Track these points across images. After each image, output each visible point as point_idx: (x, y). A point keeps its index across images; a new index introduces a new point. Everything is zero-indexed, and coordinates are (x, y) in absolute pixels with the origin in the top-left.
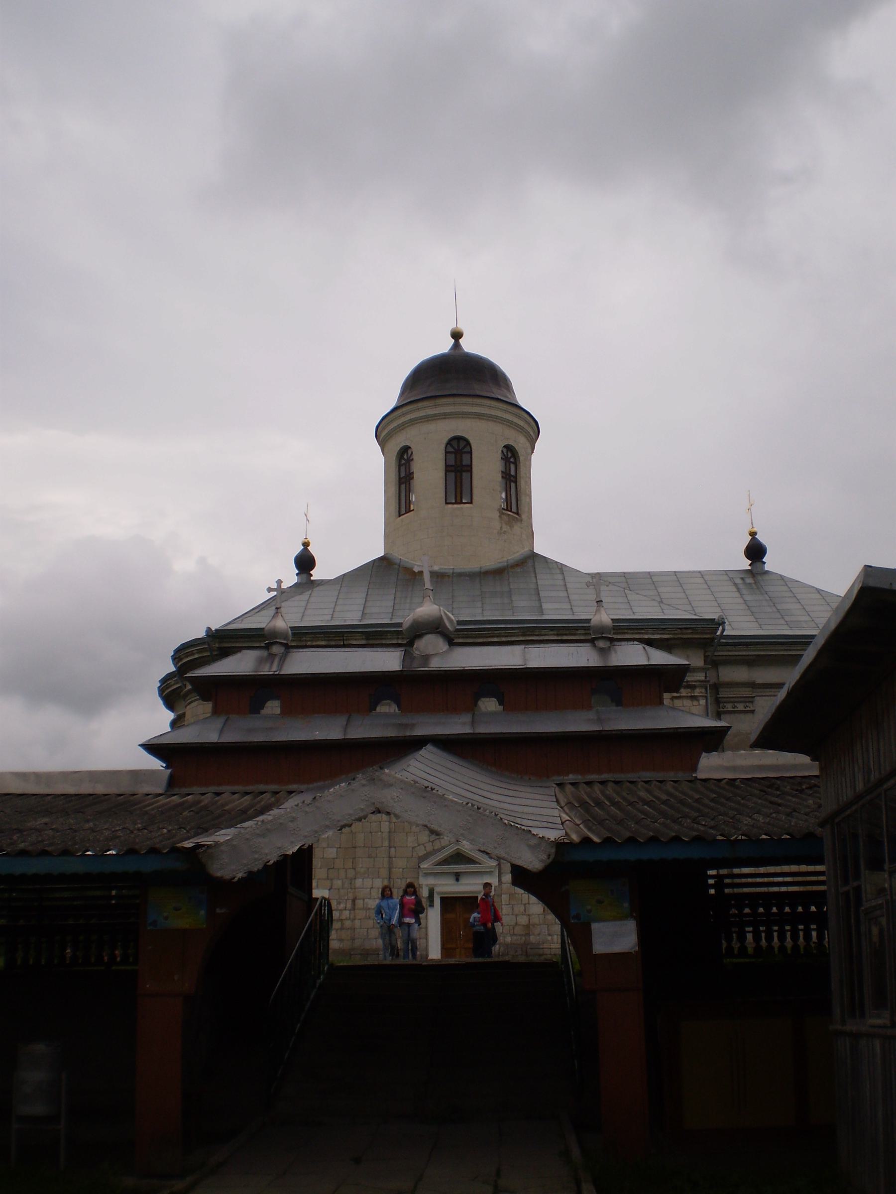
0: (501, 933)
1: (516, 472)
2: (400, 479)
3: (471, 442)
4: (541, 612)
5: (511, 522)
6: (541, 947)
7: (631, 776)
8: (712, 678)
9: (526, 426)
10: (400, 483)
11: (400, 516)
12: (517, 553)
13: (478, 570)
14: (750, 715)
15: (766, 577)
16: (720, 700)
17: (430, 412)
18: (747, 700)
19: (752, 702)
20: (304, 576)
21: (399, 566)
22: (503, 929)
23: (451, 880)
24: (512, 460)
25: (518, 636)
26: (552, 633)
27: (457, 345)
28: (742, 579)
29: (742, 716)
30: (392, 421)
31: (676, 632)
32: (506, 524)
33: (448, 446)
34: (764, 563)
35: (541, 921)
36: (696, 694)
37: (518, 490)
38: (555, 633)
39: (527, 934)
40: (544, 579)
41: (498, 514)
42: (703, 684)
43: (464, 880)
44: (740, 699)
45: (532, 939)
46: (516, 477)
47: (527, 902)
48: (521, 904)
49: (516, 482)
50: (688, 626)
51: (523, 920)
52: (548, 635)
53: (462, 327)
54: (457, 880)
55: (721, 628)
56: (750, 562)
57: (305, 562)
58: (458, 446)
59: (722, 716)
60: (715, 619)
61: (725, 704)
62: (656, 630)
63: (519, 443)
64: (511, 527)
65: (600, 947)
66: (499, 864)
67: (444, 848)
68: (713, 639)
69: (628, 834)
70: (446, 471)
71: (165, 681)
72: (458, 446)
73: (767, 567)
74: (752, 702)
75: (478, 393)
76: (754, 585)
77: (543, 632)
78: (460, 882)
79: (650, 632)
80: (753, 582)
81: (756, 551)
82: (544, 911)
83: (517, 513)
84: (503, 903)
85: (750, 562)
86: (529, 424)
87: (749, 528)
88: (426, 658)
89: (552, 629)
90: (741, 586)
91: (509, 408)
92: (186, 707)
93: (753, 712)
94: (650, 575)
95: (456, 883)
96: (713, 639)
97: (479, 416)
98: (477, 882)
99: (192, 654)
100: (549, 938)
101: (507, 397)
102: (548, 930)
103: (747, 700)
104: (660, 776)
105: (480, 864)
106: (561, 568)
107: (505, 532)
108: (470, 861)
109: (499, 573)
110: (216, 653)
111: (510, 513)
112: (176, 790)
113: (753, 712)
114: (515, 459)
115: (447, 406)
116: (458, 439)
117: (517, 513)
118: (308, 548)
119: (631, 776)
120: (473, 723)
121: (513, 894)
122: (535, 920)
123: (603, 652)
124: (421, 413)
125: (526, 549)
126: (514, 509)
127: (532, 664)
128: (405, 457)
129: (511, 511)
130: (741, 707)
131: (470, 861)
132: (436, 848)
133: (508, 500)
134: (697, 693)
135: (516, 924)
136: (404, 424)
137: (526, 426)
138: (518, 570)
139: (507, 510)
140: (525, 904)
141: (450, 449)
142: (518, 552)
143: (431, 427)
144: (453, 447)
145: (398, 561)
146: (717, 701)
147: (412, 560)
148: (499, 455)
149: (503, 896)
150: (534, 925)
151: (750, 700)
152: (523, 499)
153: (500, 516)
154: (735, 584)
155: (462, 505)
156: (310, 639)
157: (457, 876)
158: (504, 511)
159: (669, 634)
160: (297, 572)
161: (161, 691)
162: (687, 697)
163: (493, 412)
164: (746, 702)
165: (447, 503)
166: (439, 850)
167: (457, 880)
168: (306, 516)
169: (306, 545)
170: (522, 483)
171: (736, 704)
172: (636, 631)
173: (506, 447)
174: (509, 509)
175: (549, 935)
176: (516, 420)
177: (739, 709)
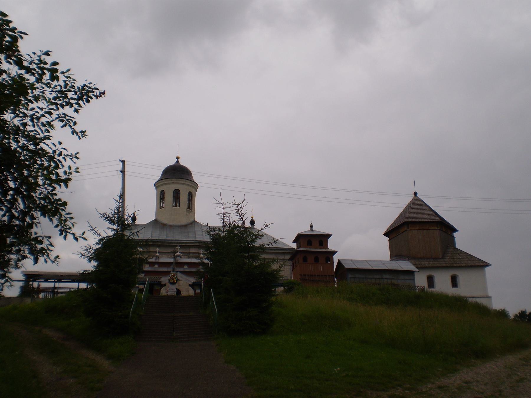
1: (191, 198)
3: (180, 190)
4: (195, 238)
5: (189, 212)
10: (161, 200)
11: (160, 208)
12: (191, 220)
13: (180, 225)
27: (178, 162)
30: (159, 183)
40: (197, 229)
46: (191, 200)
49: (191, 201)
53: (179, 156)
63: (192, 190)
65: (196, 292)
77: (196, 243)
83: (191, 210)
86: (196, 185)
87: (251, 216)
88: (178, 260)
89: (198, 243)
97: (183, 184)
101: (190, 178)
107: (188, 215)
109: (186, 226)
111: (189, 210)
115: (174, 181)
116: (177, 189)
125: (193, 219)
128: (162, 192)
129: (189, 209)
133: (189, 204)
136: (162, 184)
138: (191, 225)
139: (189, 209)
145: (159, 221)
148: (187, 195)
165: (173, 207)
170: (193, 202)
173: (190, 192)
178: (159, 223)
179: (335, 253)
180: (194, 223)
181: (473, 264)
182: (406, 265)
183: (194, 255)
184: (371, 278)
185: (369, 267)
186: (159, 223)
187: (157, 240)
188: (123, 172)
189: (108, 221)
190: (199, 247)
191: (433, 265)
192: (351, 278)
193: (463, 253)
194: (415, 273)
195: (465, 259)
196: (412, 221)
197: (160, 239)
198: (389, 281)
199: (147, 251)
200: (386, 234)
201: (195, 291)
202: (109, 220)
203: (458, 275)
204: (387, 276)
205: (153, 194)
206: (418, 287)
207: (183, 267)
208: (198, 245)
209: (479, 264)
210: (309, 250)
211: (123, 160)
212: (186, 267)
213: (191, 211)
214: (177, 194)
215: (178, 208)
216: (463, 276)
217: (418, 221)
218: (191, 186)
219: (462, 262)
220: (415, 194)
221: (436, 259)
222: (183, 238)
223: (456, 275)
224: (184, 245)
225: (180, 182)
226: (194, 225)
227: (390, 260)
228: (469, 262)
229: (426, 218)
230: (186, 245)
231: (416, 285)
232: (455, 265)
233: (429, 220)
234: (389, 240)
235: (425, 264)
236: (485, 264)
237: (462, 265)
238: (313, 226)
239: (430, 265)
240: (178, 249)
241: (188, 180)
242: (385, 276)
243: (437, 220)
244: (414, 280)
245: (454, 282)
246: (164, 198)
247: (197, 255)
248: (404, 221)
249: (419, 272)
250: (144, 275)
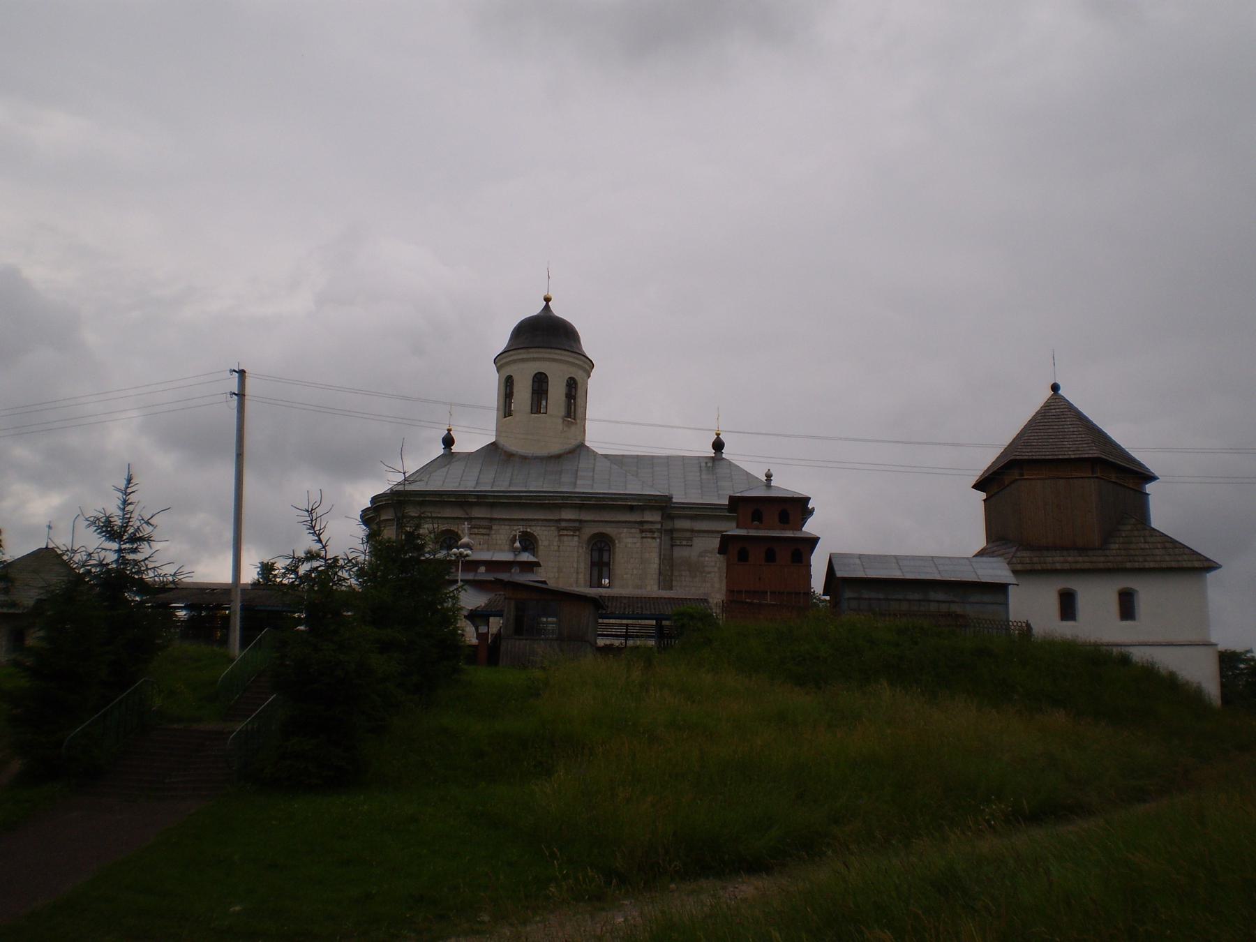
2: (506, 394)
5: (569, 424)
8: (668, 525)
10: (506, 398)
11: (505, 417)
12: (573, 443)
13: (546, 455)
14: (688, 548)
17: (525, 356)
24: (574, 386)
25: (559, 500)
27: (547, 307)
28: (706, 463)
29: (685, 548)
30: (502, 359)
36: (655, 536)
42: (660, 531)
49: (575, 399)
53: (551, 294)
57: (448, 441)
63: (578, 375)
65: (480, 631)
70: (533, 393)
71: (365, 511)
73: (724, 456)
81: (718, 445)
83: (574, 419)
86: (585, 362)
91: (575, 355)
94: (653, 457)
97: (554, 360)
99: (382, 501)
109: (558, 457)
111: (569, 419)
115: (534, 353)
124: (520, 357)
126: (573, 417)
127: (494, 559)
129: (570, 418)
130: (684, 543)
134: (656, 535)
139: (566, 417)
141: (536, 380)
144: (537, 378)
146: (672, 539)
151: (690, 539)
154: (700, 467)
155: (541, 415)
158: (566, 419)
161: (362, 517)
162: (649, 537)
163: (563, 358)
165: (532, 413)
169: (449, 430)
170: (579, 400)
173: (570, 378)
176: (577, 362)
178: (500, 450)
179: (813, 542)
180: (581, 448)
181: (1174, 564)
182: (996, 571)
183: (572, 524)
184: (900, 600)
185: (896, 574)
187: (486, 491)
188: (241, 395)
189: (104, 534)
190: (581, 507)
191: (1074, 566)
192: (849, 599)
193: (1158, 534)
194: (1010, 587)
195: (1157, 552)
196: (1031, 457)
197: (495, 489)
198: (944, 608)
199: (467, 516)
200: (978, 486)
201: (477, 629)
202: (104, 532)
203: (1137, 591)
204: (940, 596)
205: (491, 381)
206: (1019, 624)
207: (476, 570)
208: (580, 502)
209: (1189, 565)
210: (753, 533)
211: (241, 368)
212: (482, 569)
213: (573, 421)
214: (540, 384)
215: (544, 415)
216: (1149, 593)
217: (1043, 457)
219: (1148, 559)
220: (1055, 388)
221: (1083, 550)
222: (547, 487)
223: (1133, 590)
224: (547, 502)
225: (546, 356)
227: (981, 553)
228: (1167, 558)
229: (1067, 449)
230: (551, 502)
231: (1011, 618)
232: (1129, 565)
233: (1073, 457)
234: (984, 500)
235: (1054, 563)
236: (1206, 564)
237: (1147, 567)
238: (771, 476)
239: (1067, 566)
240: (466, 529)
241: (565, 350)
242: (933, 595)
243: (1090, 456)
244: (1006, 604)
245: (1127, 606)
247: (577, 524)
248: (1011, 458)
249: (1017, 585)
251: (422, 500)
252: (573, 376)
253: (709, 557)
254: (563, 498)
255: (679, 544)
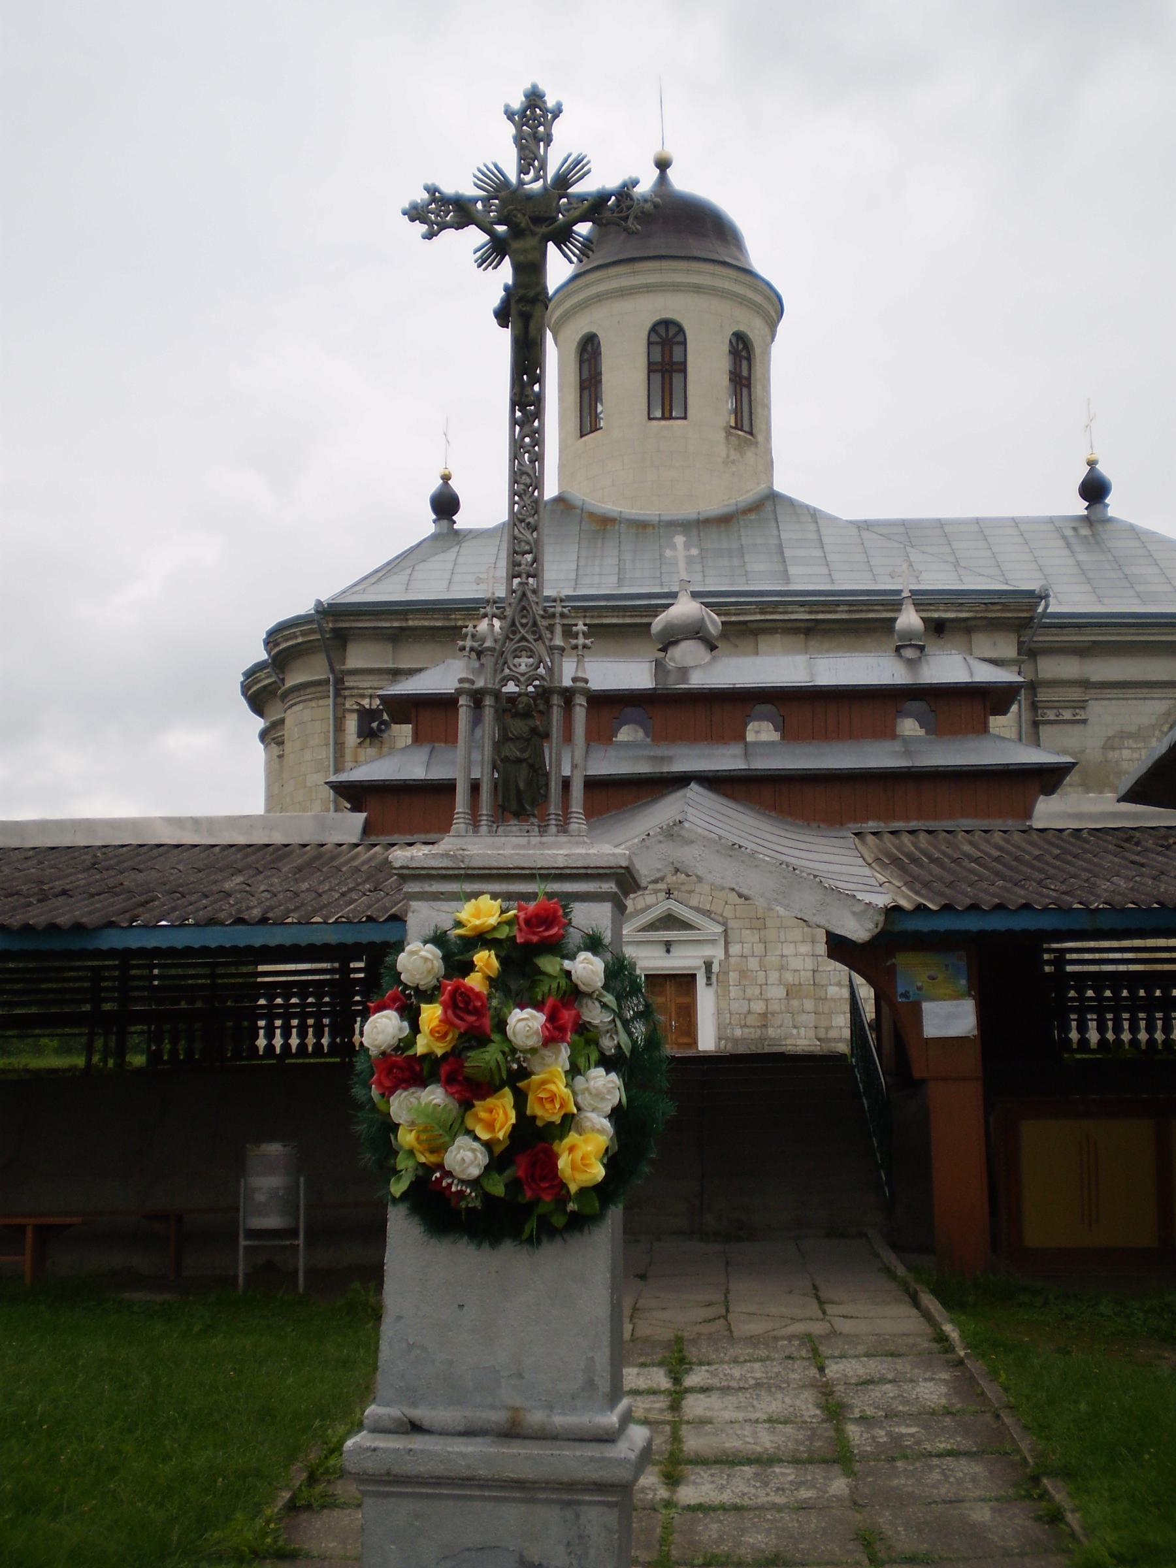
0: (728, 1024)
2: (582, 382)
4: (787, 578)
6: (784, 1043)
7: (949, 824)
9: (765, 304)
10: (582, 389)
11: (582, 436)
13: (694, 516)
14: (1081, 727)
15: (1108, 527)
16: (1038, 704)
17: (626, 282)
18: (1075, 704)
19: (1084, 708)
20: (445, 523)
21: (582, 509)
22: (730, 1019)
23: (660, 951)
24: (744, 353)
25: (755, 613)
26: (802, 609)
27: (663, 179)
28: (1075, 529)
31: (978, 608)
32: (735, 449)
33: (652, 332)
34: (1107, 506)
35: (783, 1008)
37: (753, 398)
38: (807, 609)
39: (764, 1025)
40: (789, 532)
41: (724, 434)
43: (676, 951)
44: (1067, 704)
45: (771, 1032)
46: (749, 379)
47: (764, 982)
48: (756, 985)
49: (749, 387)
50: (997, 601)
51: (758, 1007)
52: (797, 612)
54: (668, 951)
55: (1043, 602)
56: (1087, 503)
58: (667, 334)
59: (1041, 727)
60: (1035, 590)
61: (1045, 711)
62: (948, 605)
63: (754, 328)
64: (742, 454)
65: (931, 1029)
66: (725, 931)
67: (648, 907)
68: (1031, 619)
69: (968, 902)
70: (650, 371)
71: (251, 674)
72: (667, 334)
74: (1084, 708)
75: (697, 254)
76: (1091, 538)
77: (790, 608)
78: (671, 954)
79: (941, 608)
80: (1090, 533)
82: (787, 995)
83: (751, 433)
84: (731, 983)
85: (1087, 503)
87: (1085, 456)
88: (684, 672)
89: (802, 604)
90: (1073, 541)
92: (285, 712)
93: (1084, 721)
94: (940, 524)
95: (667, 955)
96: (1031, 619)
97: (698, 289)
98: (696, 954)
100: (795, 1031)
102: (793, 1020)
103: (1075, 704)
104: (985, 824)
105: (699, 930)
106: (814, 515)
107: (733, 462)
108: (686, 925)
109: (725, 521)
110: (328, 636)
111: (740, 433)
112: (373, 839)
113: (1084, 721)
114: (749, 352)
115: (648, 273)
116: (667, 323)
117: (751, 433)
118: (449, 482)
119: (949, 824)
120: (746, 755)
121: (744, 971)
122: (775, 1007)
123: (912, 664)
124: (614, 284)
125: (763, 486)
126: (746, 428)
128: (589, 348)
129: (741, 430)
130: (1067, 715)
131: (686, 925)
132: (639, 907)
133: (737, 412)
135: (749, 1012)
137: (765, 304)
138: (753, 516)
139: (736, 428)
140: (761, 985)
141: (655, 338)
142: (751, 490)
143: (626, 305)
145: (580, 504)
147: (600, 502)
148: (726, 348)
149: (731, 973)
150: (773, 1014)
151: (1082, 705)
152: (758, 411)
153: (727, 438)
154: (1064, 537)
156: (462, 617)
157: (668, 946)
158: (733, 431)
159: (968, 611)
160: (434, 517)
161: (245, 689)
164: (1075, 708)
165: (650, 419)
166: (643, 910)
167: (668, 951)
168: (445, 435)
169: (446, 478)
171: (1060, 710)
172: (921, 608)
174: (739, 427)
175: (795, 1027)
177: (1065, 718)
186: (578, 511)
208: (807, 617)
213: (749, 437)
218: (743, 301)
226: (775, 512)
230: (733, 619)
240: (682, 565)
246: (600, 373)
250: (367, 829)
251: (400, 628)
252: (742, 328)
253: (1133, 750)
254: (763, 608)
255: (1052, 718)
